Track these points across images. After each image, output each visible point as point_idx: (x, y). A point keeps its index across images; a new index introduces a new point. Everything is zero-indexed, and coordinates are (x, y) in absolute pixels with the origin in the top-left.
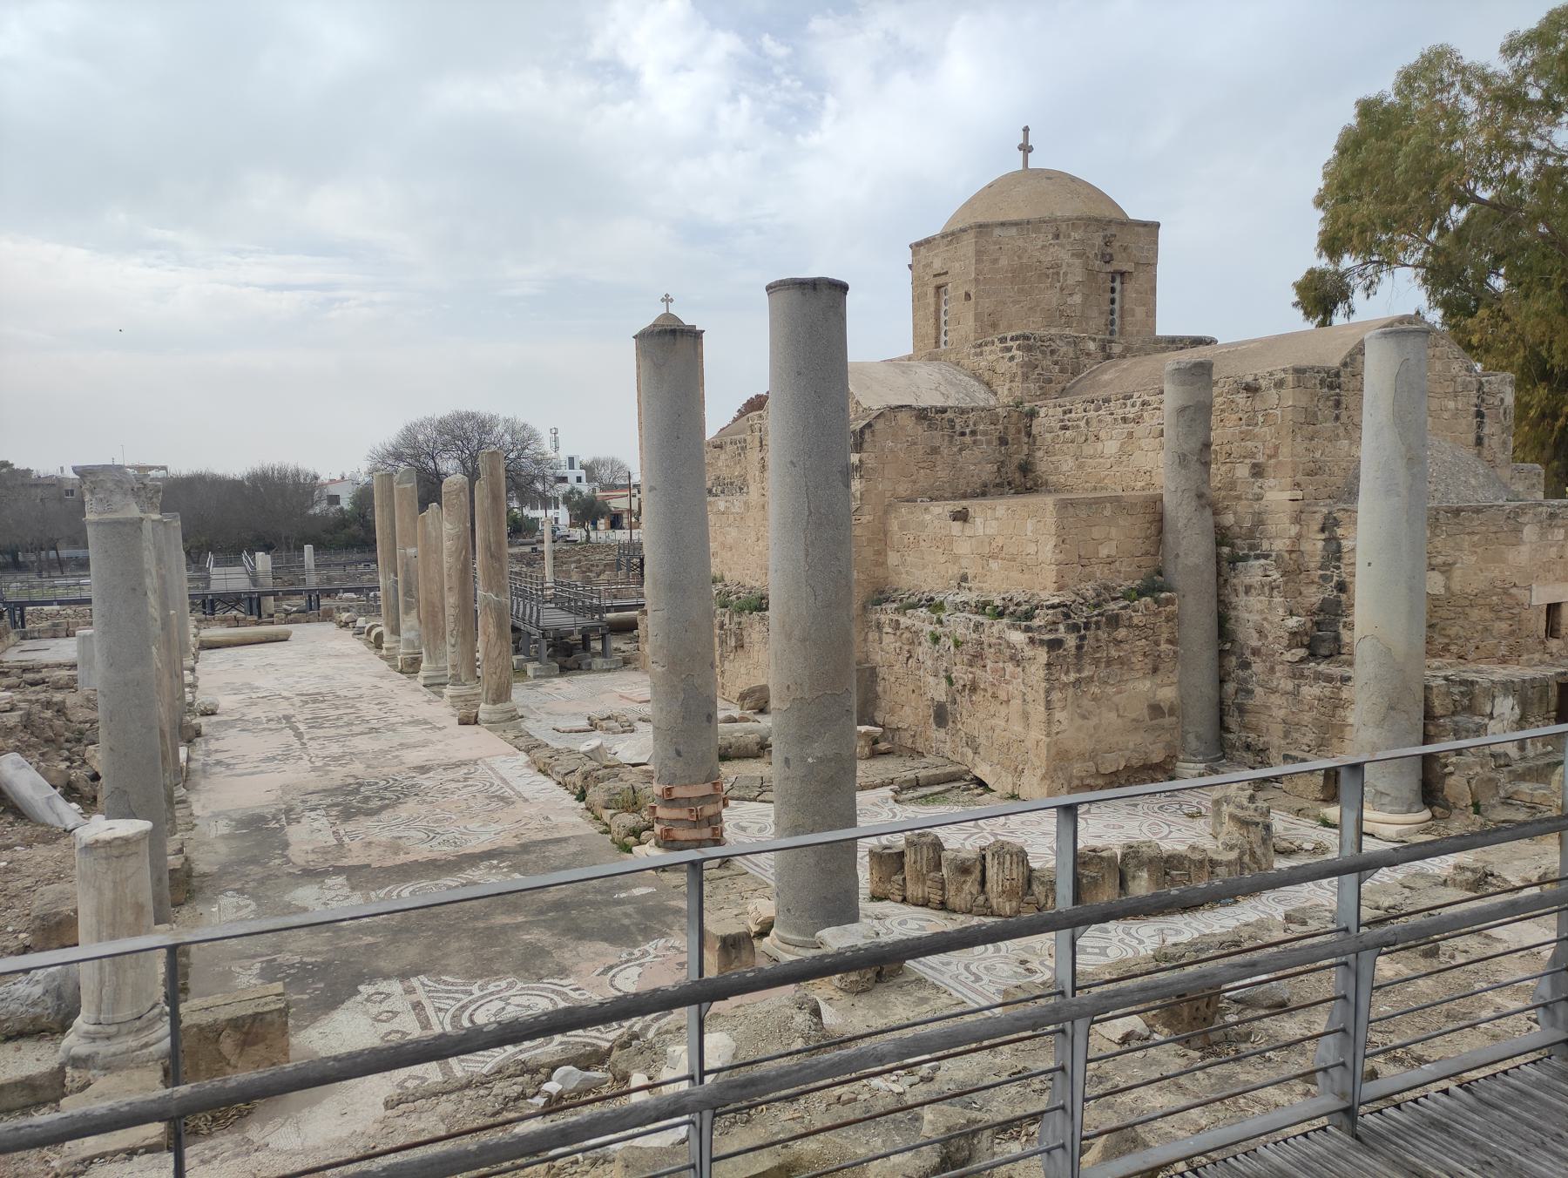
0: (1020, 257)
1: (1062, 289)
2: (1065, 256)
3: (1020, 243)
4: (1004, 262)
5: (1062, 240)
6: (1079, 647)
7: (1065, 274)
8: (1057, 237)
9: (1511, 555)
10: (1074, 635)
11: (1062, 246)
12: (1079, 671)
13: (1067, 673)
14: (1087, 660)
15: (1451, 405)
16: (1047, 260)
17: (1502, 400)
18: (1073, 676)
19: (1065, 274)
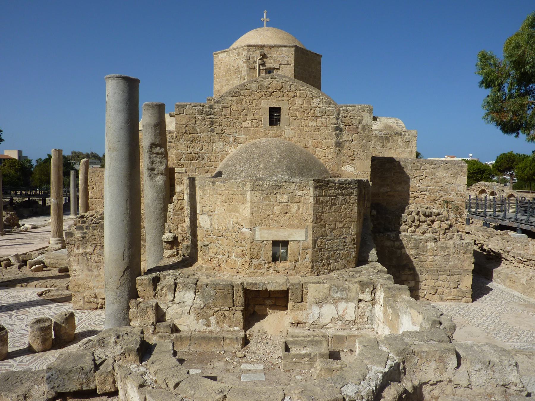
0: (227, 66)
1: (240, 78)
2: (241, 63)
3: (227, 59)
4: (222, 68)
5: (241, 56)
6: (83, 238)
7: (241, 71)
8: (239, 55)
9: (241, 208)
10: (80, 231)
11: (240, 59)
12: (84, 248)
13: (78, 248)
14: (89, 243)
15: (311, 123)
16: (236, 66)
17: (361, 121)
18: (81, 251)
19: (241, 71)
